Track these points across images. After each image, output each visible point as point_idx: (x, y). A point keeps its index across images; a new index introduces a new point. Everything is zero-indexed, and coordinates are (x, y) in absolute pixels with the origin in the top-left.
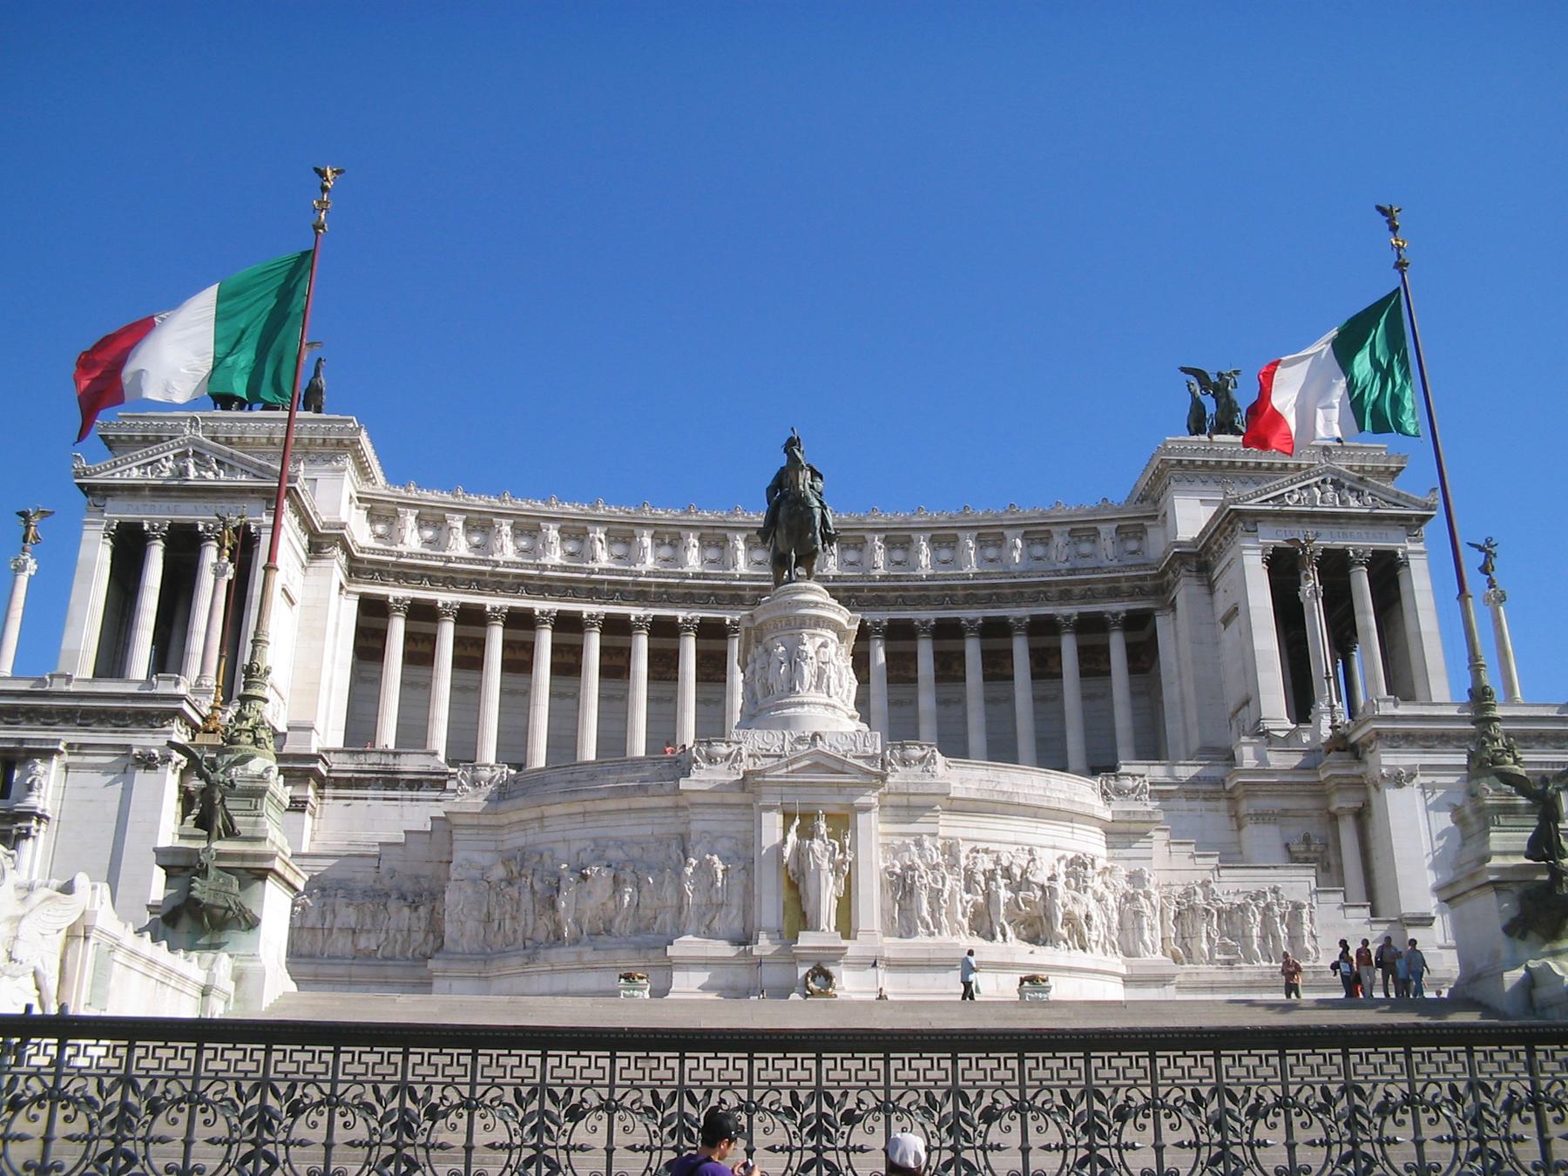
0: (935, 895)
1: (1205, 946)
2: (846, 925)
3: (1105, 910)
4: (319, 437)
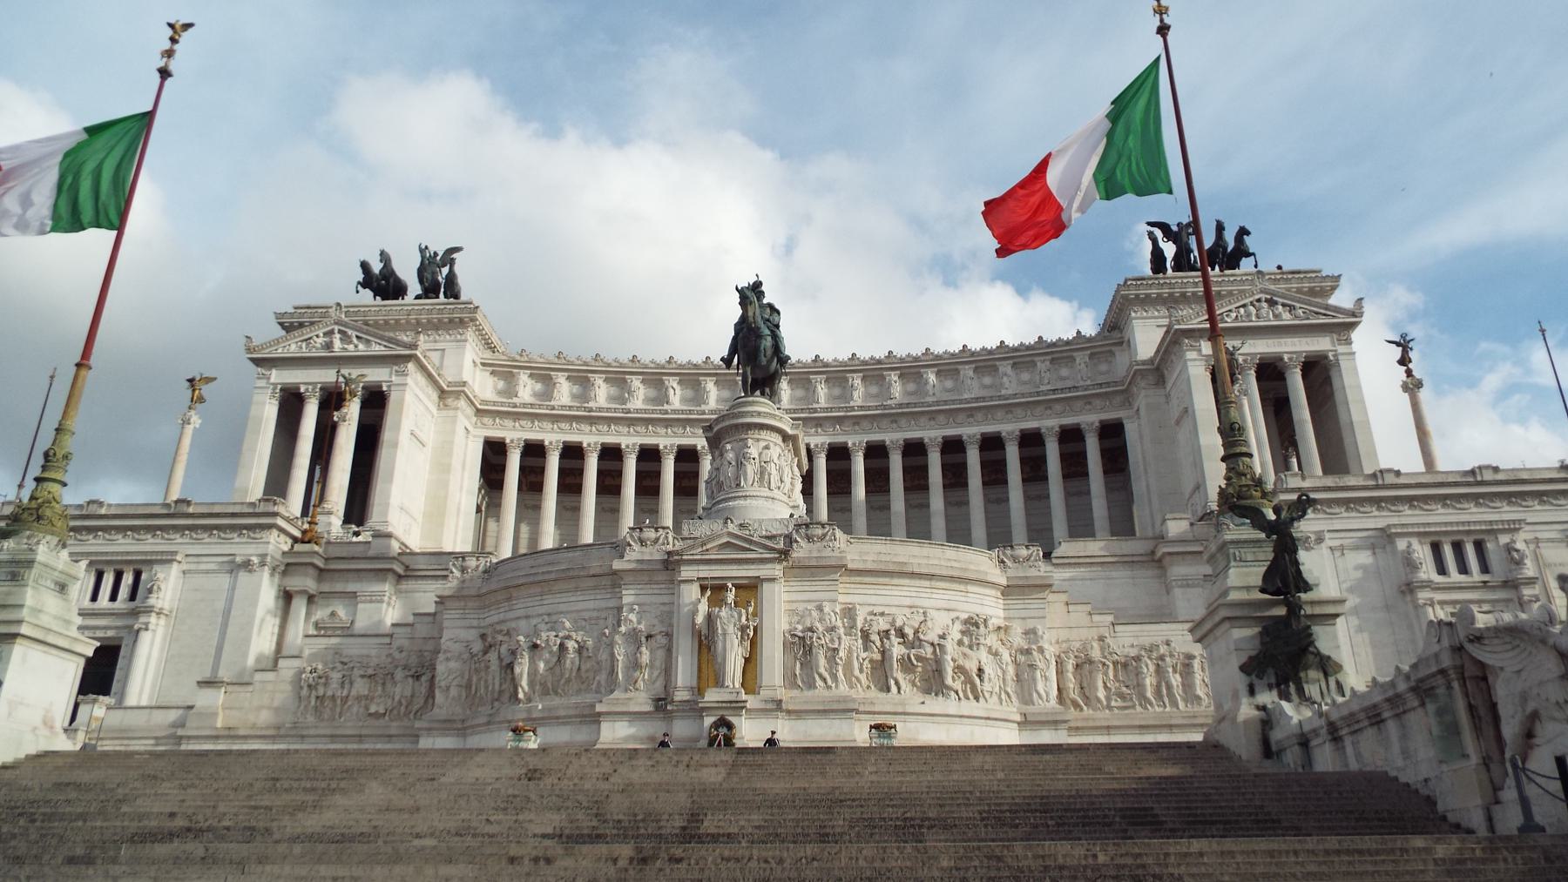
1: (1101, 694)
3: (1000, 663)
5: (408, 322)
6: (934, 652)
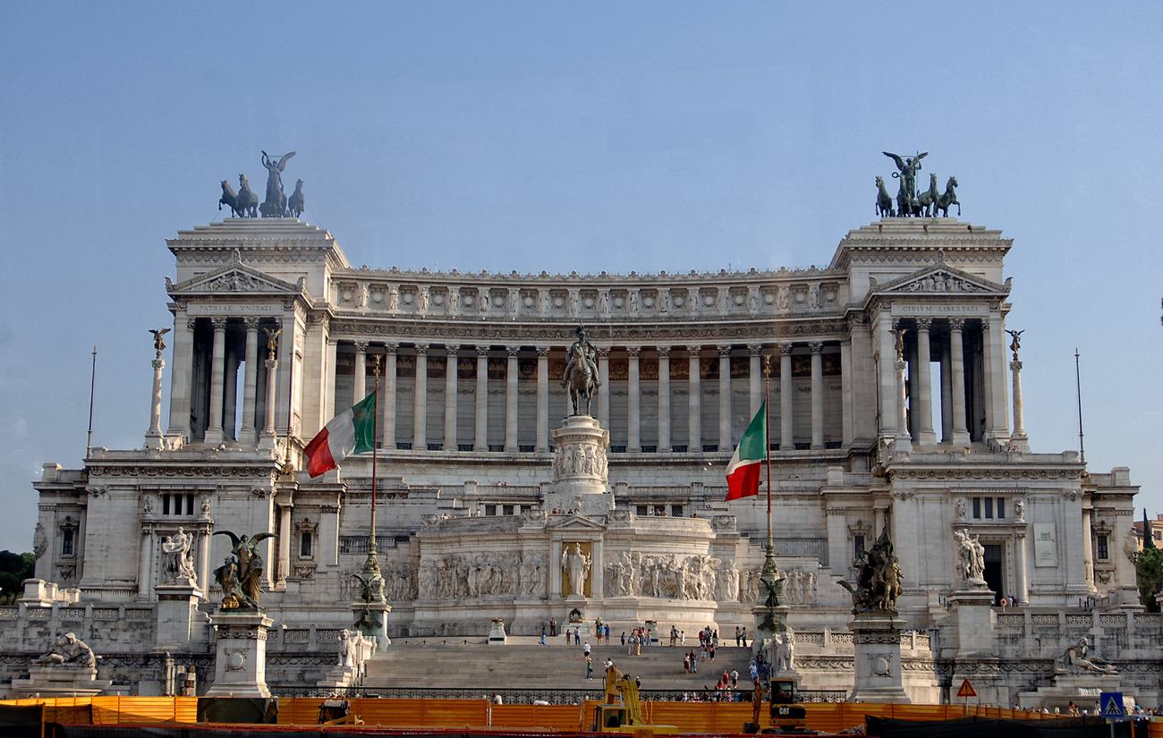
0: (627, 579)
2: (587, 593)
4: (307, 246)
5: (277, 249)
6: (676, 577)
